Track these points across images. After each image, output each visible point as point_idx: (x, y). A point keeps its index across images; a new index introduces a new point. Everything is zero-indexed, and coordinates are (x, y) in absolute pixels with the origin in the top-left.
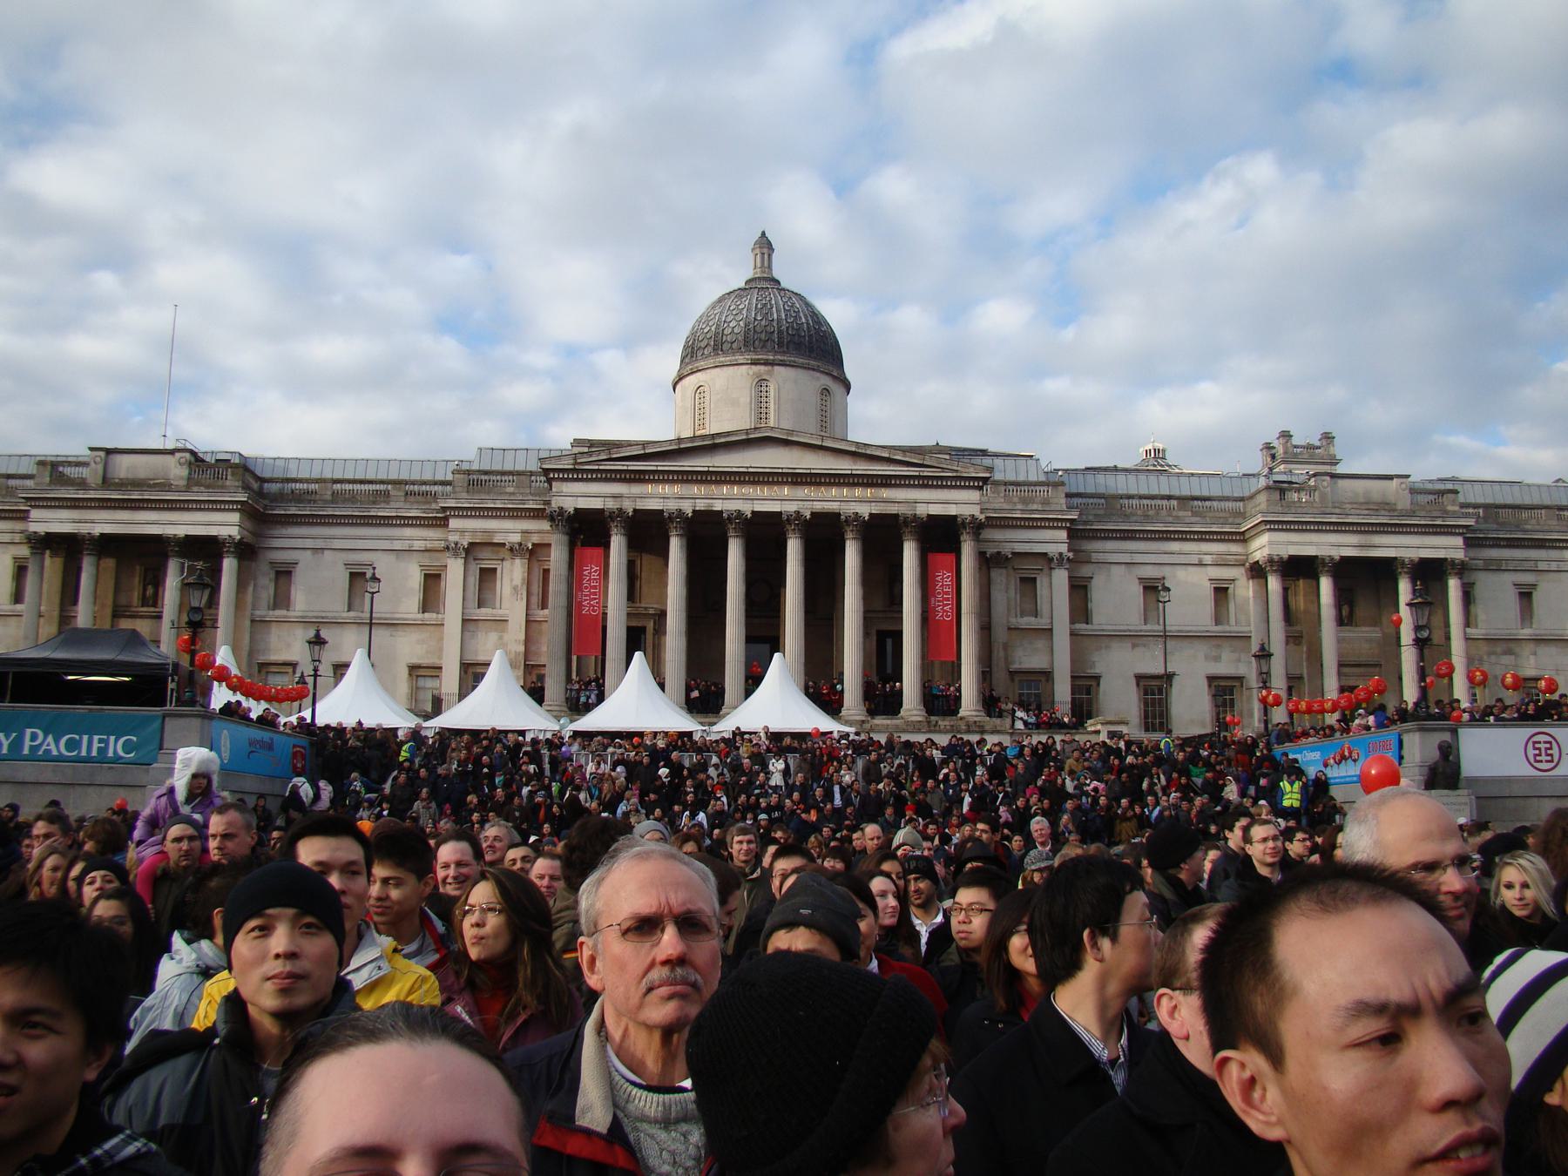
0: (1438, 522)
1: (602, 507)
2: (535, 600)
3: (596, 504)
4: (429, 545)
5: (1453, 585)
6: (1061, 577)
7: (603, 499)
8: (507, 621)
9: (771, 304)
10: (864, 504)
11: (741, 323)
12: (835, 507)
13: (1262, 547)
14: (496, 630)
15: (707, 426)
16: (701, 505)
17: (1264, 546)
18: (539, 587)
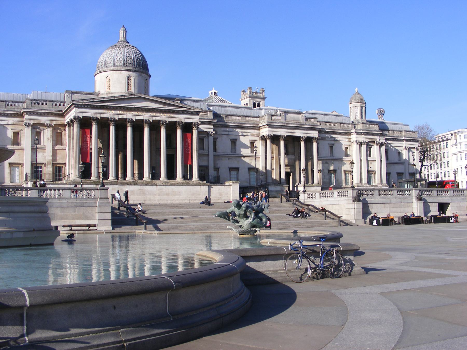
0: (312, 127)
1: (90, 116)
2: (54, 142)
3: (89, 115)
4: (15, 123)
5: (315, 144)
6: (211, 139)
7: (90, 114)
8: (46, 149)
9: (130, 51)
10: (166, 118)
11: (122, 57)
12: (160, 119)
13: (265, 132)
14: (42, 152)
15: (111, 89)
16: (120, 117)
17: (266, 131)
18: (55, 138)
